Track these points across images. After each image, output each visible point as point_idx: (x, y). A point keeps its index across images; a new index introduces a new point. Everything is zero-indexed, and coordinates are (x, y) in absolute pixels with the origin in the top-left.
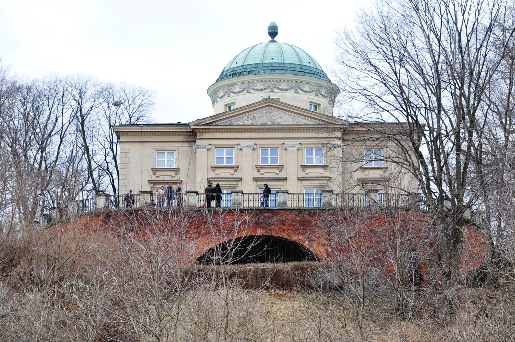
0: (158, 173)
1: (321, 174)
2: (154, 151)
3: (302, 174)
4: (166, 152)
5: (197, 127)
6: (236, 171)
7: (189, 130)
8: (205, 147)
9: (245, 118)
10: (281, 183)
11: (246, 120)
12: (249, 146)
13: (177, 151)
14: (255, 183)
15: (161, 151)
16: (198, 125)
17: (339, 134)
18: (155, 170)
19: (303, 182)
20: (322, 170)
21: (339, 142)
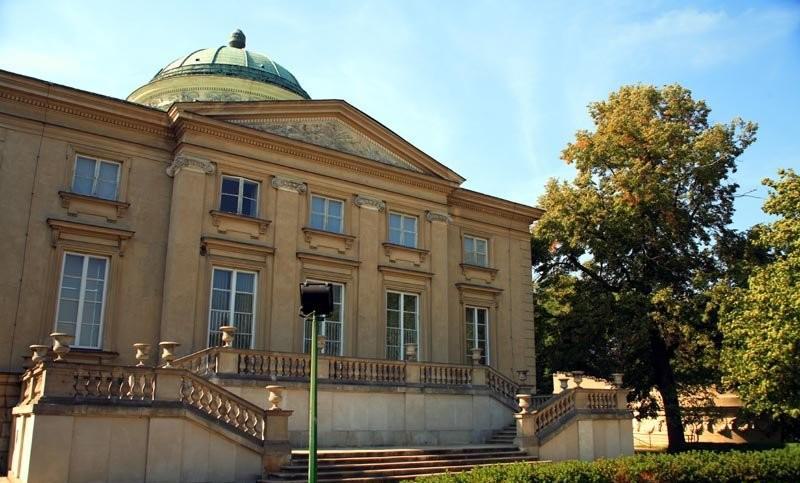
0: (75, 206)
1: (416, 265)
2: (70, 152)
3: (385, 261)
4: (99, 161)
5: (190, 117)
6: (263, 232)
7: (163, 124)
8: (203, 166)
9: (289, 127)
10: (348, 272)
11: (290, 130)
12: (292, 184)
13: (128, 164)
14: (299, 264)
15: (88, 155)
16: (194, 113)
17: (443, 198)
18: (65, 197)
19: (386, 278)
20: (416, 259)
21: (443, 212)
